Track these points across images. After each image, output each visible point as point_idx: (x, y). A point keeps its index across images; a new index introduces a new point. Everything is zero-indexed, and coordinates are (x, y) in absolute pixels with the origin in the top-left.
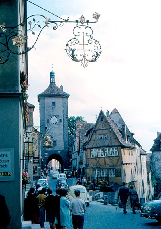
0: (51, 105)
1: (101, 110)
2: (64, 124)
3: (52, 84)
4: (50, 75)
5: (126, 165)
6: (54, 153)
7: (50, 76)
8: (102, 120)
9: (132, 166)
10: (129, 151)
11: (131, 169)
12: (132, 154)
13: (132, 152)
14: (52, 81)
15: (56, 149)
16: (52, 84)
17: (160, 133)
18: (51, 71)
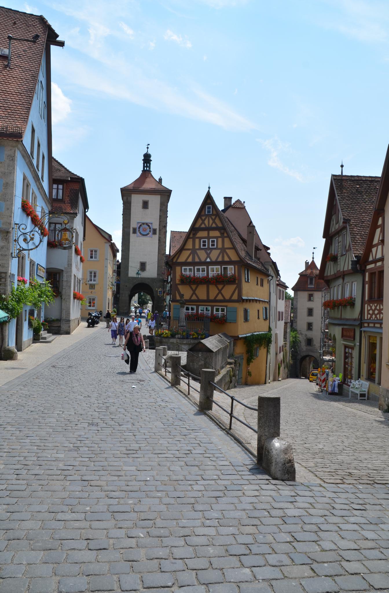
0: (141, 204)
1: (209, 192)
2: (159, 238)
3: (146, 173)
4: (143, 158)
5: (248, 301)
6: (140, 282)
7: (143, 160)
8: (209, 212)
9: (260, 307)
10: (257, 278)
11: (258, 311)
12: (262, 285)
13: (262, 281)
14: (147, 169)
15: (144, 275)
16: (146, 173)
17: (309, 264)
18: (145, 152)
